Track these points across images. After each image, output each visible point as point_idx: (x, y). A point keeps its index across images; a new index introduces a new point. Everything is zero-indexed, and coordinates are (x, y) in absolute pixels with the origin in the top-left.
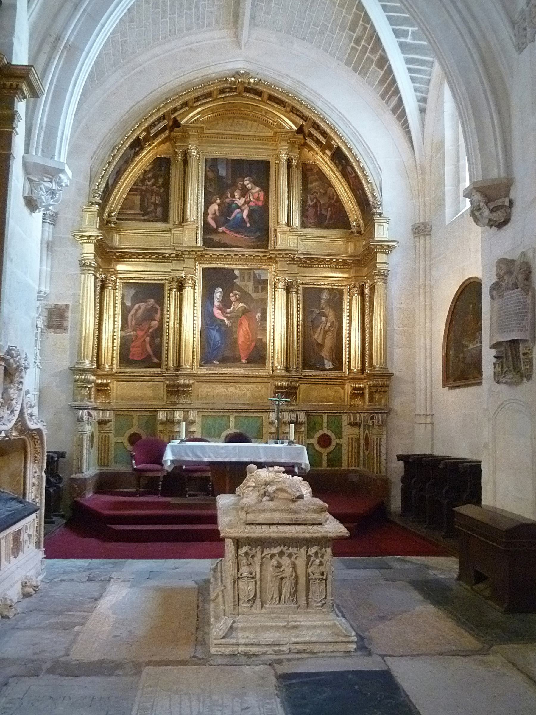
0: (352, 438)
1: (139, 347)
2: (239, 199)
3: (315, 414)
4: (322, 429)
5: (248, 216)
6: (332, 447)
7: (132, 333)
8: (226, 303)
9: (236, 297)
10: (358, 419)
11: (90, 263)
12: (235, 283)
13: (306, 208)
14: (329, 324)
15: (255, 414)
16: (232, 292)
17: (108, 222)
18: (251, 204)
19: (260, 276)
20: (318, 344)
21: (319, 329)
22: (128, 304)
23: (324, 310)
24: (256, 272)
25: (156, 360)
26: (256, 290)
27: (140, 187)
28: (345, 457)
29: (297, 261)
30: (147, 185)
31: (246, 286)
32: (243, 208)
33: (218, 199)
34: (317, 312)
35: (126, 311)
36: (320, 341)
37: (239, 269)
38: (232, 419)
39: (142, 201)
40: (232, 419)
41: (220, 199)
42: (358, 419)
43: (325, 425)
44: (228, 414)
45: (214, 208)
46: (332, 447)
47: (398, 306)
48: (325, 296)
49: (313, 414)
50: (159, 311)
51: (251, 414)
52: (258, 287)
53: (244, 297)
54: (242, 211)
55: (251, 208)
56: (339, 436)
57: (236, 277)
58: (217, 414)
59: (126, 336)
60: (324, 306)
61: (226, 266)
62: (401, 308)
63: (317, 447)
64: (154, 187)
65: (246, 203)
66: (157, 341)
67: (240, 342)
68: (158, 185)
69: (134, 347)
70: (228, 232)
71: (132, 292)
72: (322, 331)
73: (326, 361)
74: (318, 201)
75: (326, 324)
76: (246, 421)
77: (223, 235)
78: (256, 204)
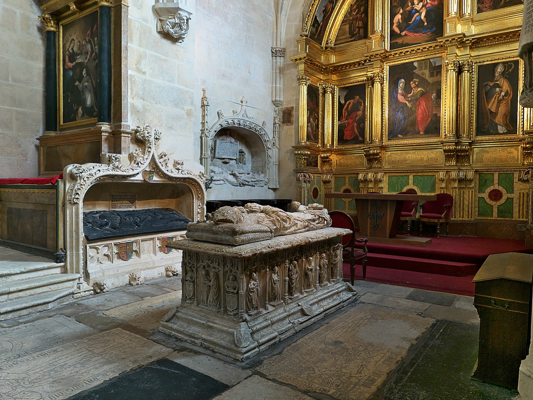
1: (350, 130)
2: (418, 4)
3: (486, 172)
4: (493, 185)
5: (425, 17)
6: (503, 201)
7: (345, 121)
8: (407, 89)
9: (415, 84)
11: (302, 77)
12: (414, 73)
15: (430, 174)
16: (412, 80)
17: (326, 48)
18: (428, 6)
19: (435, 63)
22: (343, 102)
24: (431, 60)
25: (360, 139)
26: (432, 75)
27: (349, 18)
28: (516, 210)
30: (353, 15)
31: (423, 74)
32: (421, 11)
33: (401, 9)
35: (341, 106)
37: (417, 61)
38: (411, 177)
39: (350, 28)
40: (411, 177)
41: (402, 9)
43: (496, 181)
44: (408, 174)
45: (399, 17)
46: (503, 201)
49: (484, 172)
50: (362, 104)
51: (426, 174)
52: (434, 72)
53: (423, 82)
54: (421, 14)
55: (428, 9)
56: (510, 190)
57: (415, 68)
58: (400, 174)
59: (342, 124)
61: (407, 61)
63: (488, 200)
64: (358, 15)
65: (423, 6)
66: (361, 125)
67: (419, 119)
68: (360, 13)
69: (346, 131)
70: (408, 34)
71: (345, 93)
76: (422, 179)
77: (406, 37)
78: (432, 5)
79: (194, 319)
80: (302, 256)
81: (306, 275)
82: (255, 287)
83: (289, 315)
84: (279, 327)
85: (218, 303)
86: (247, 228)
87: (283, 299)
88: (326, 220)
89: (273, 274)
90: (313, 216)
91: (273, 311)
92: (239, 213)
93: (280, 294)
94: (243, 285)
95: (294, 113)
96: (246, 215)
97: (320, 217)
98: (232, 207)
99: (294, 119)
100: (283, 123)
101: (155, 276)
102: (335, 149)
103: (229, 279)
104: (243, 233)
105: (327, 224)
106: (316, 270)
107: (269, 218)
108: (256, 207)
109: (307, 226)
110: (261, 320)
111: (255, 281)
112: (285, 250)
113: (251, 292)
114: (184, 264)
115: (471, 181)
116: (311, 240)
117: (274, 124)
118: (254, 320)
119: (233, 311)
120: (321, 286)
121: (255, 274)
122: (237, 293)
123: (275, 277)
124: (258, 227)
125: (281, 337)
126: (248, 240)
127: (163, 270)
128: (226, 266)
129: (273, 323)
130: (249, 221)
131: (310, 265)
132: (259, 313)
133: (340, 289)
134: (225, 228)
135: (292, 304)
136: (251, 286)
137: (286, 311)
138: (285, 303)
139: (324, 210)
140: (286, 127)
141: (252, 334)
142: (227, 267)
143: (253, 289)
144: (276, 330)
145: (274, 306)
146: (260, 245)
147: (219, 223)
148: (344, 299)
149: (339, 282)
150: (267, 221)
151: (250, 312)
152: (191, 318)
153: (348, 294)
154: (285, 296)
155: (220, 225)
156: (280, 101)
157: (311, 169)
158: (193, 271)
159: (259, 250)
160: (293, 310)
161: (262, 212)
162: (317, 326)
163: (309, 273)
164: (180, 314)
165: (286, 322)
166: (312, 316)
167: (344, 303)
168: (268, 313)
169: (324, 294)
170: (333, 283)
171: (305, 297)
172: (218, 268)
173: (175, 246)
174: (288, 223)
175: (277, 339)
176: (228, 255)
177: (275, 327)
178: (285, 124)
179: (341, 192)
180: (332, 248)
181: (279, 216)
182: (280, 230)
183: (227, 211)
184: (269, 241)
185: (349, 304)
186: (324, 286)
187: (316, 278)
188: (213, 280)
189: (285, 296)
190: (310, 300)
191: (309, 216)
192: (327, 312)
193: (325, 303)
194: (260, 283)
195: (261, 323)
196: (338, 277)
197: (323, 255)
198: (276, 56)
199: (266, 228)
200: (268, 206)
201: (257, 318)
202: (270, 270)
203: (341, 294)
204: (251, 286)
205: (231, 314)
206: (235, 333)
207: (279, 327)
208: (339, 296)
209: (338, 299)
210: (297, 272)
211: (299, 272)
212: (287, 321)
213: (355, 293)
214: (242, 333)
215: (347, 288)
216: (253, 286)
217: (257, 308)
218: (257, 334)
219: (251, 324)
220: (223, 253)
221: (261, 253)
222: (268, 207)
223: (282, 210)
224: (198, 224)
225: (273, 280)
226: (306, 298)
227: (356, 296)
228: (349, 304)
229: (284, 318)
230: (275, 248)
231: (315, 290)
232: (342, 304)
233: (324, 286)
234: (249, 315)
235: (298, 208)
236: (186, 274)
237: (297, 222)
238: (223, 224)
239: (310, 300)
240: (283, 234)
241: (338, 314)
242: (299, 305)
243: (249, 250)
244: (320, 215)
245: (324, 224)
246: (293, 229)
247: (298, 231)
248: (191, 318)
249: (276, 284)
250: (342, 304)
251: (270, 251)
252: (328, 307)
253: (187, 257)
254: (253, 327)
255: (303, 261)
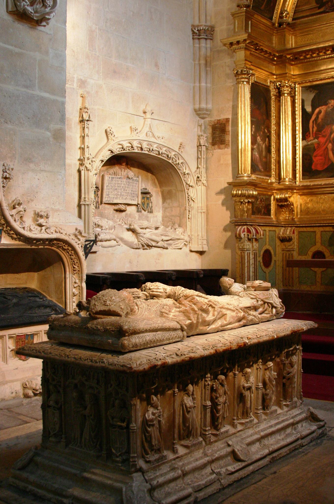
1: (321, 156)
7: (314, 141)
11: (242, 71)
22: (309, 109)
35: (306, 116)
59: (308, 145)
69: (315, 157)
79: (62, 467)
80: (234, 367)
81: (241, 398)
82: (156, 418)
83: (212, 462)
84: (195, 480)
85: (98, 443)
86: (142, 326)
87: (203, 435)
88: (276, 308)
89: (185, 398)
90: (253, 301)
91: (186, 454)
92: (130, 300)
93: (197, 429)
94: (136, 414)
95: (230, 128)
96: (142, 303)
97: (265, 303)
98: (119, 290)
99: (229, 138)
100: (213, 144)
101: (5, 396)
102: (299, 186)
103: (113, 406)
104: (135, 332)
105: (277, 313)
106: (257, 389)
107: (179, 308)
108: (158, 289)
109: (244, 318)
110: (165, 468)
111: (156, 407)
112: (204, 359)
113: (149, 426)
114: (45, 379)
116: (247, 342)
117: (198, 146)
118: (155, 469)
119: (120, 455)
120: (266, 414)
121: (155, 398)
122: (128, 427)
123: (188, 402)
124: (160, 322)
125: (198, 496)
126: (144, 343)
127: (18, 387)
128: (109, 385)
129: (185, 474)
130: (146, 313)
131: (247, 380)
132: (164, 457)
133: (298, 419)
134: (107, 324)
135: (216, 444)
136: (149, 416)
137: (206, 455)
138: (205, 442)
139: (272, 291)
140: (217, 152)
141: (151, 490)
142: (111, 387)
143: (152, 420)
144: (190, 484)
145: (186, 447)
146: (164, 351)
147: (98, 316)
148: (303, 433)
149: (295, 407)
150: (174, 313)
151: (147, 458)
152: (56, 465)
153: (311, 425)
154: (206, 431)
155: (100, 320)
156: (207, 110)
157: (259, 219)
158: (59, 392)
159: (160, 359)
160: (218, 453)
161: (169, 297)
162: (257, 477)
163: (247, 393)
164: (40, 458)
165: (206, 471)
166: (249, 462)
167: (303, 441)
168: (178, 458)
169: (271, 426)
170: (286, 409)
171: (239, 431)
172: (97, 389)
173: (30, 352)
174: (211, 314)
175: (191, 499)
176: (111, 367)
177: (188, 479)
178: (216, 146)
179: (308, 258)
180: (283, 352)
181: (195, 304)
182: (197, 326)
183: (111, 298)
184: (179, 345)
185: (311, 441)
186: (272, 413)
187: (257, 403)
188: (88, 407)
189: (206, 431)
190: (248, 437)
191: (247, 302)
192: (274, 455)
193: (272, 441)
194: (163, 411)
195: (166, 474)
196: (295, 399)
197: (270, 365)
198: (199, 39)
199: (173, 324)
200: (179, 287)
201: (159, 466)
202: (180, 390)
203: (299, 425)
204: (149, 415)
205: (118, 459)
206: (124, 489)
207: (195, 480)
208: (295, 429)
209: (293, 434)
210: (225, 393)
211: (229, 393)
212: (208, 470)
213: (322, 423)
214: (135, 489)
215: (309, 416)
216: (151, 417)
217: (159, 451)
218: (159, 492)
219: (150, 475)
220: (103, 365)
221: (165, 366)
222: (180, 290)
223: (201, 294)
224: (65, 318)
225: (186, 406)
226: (240, 433)
227: (323, 429)
228: (311, 441)
229: (204, 466)
230: (187, 356)
231: (256, 421)
232: (299, 442)
233: (272, 413)
234: (147, 462)
235: (230, 287)
236: (48, 397)
237: (225, 313)
238: (104, 318)
239: (248, 437)
240: (203, 332)
241: (292, 457)
242: (229, 445)
243: (145, 361)
244: (266, 298)
245: (272, 313)
246: (219, 323)
247: (228, 326)
248: (56, 465)
249: (190, 413)
250: (299, 442)
251: (179, 361)
252: (276, 447)
253: (49, 370)
254: (152, 479)
255: (235, 374)
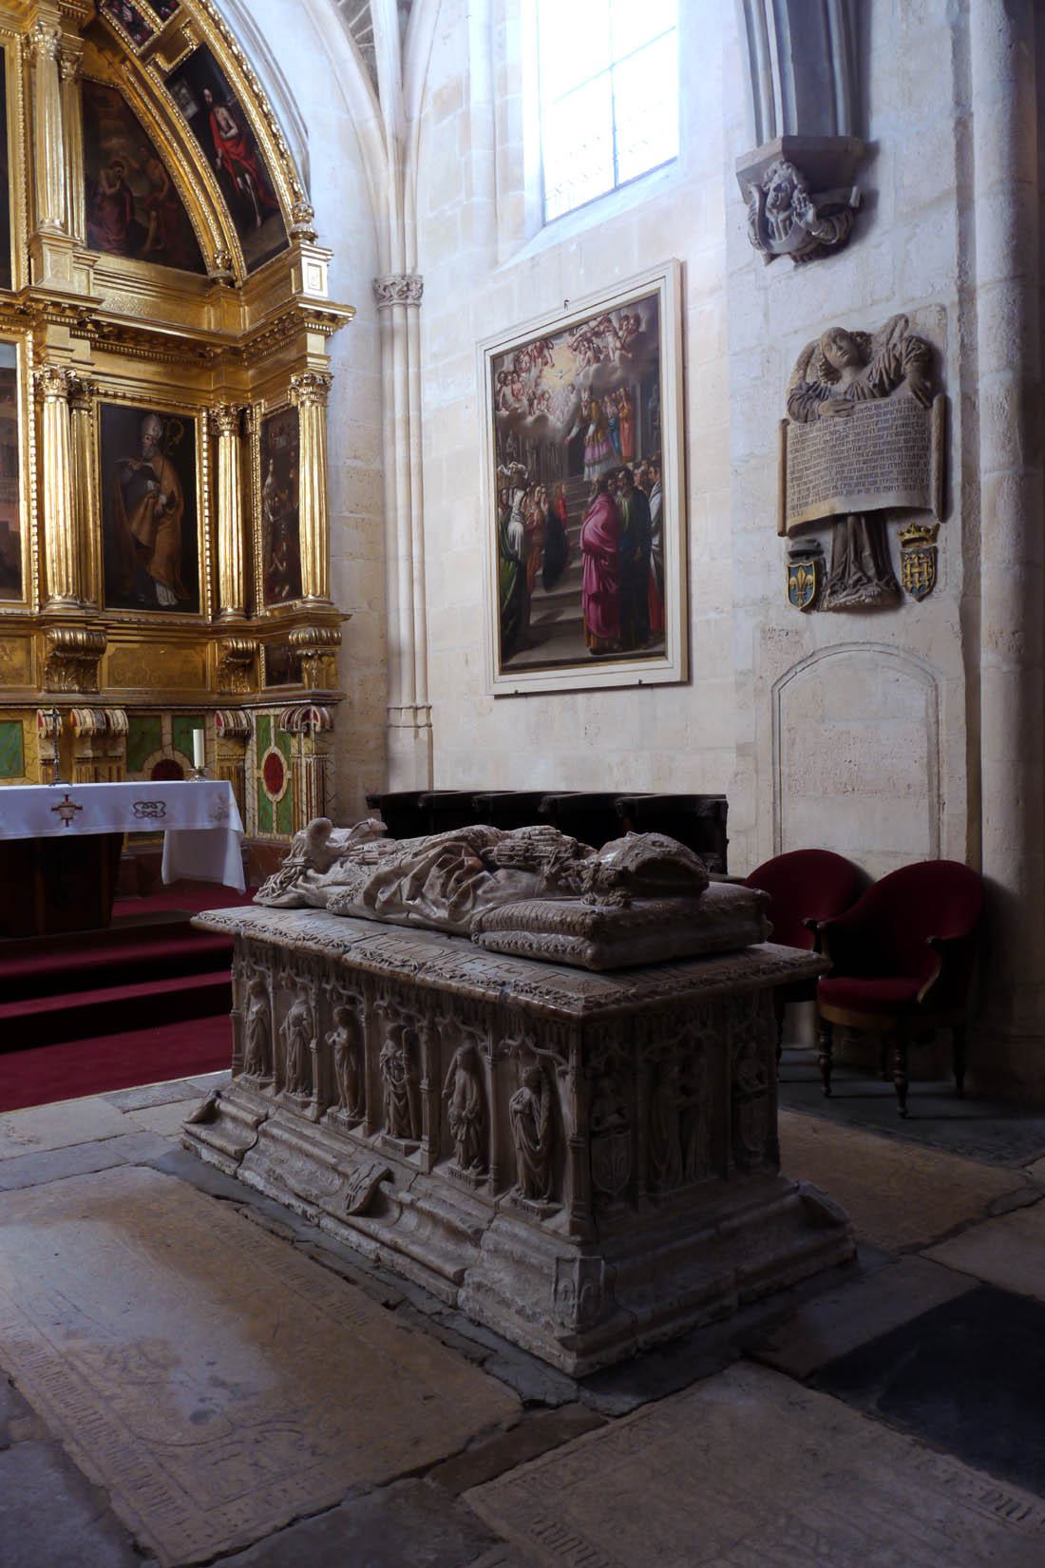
0: (228, 768)
4: (161, 748)
10: (244, 722)
13: (98, 199)
14: (163, 499)
20: (138, 544)
21: (142, 510)
23: (150, 465)
29: (91, 331)
34: (135, 467)
36: (143, 538)
42: (244, 722)
43: (167, 738)
47: (349, 462)
48: (152, 429)
60: (151, 454)
62: (354, 469)
72: (149, 514)
73: (159, 589)
74: (125, 188)
75: (156, 498)
115: (117, 735)
